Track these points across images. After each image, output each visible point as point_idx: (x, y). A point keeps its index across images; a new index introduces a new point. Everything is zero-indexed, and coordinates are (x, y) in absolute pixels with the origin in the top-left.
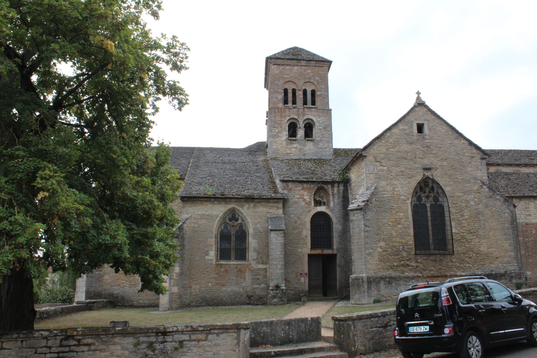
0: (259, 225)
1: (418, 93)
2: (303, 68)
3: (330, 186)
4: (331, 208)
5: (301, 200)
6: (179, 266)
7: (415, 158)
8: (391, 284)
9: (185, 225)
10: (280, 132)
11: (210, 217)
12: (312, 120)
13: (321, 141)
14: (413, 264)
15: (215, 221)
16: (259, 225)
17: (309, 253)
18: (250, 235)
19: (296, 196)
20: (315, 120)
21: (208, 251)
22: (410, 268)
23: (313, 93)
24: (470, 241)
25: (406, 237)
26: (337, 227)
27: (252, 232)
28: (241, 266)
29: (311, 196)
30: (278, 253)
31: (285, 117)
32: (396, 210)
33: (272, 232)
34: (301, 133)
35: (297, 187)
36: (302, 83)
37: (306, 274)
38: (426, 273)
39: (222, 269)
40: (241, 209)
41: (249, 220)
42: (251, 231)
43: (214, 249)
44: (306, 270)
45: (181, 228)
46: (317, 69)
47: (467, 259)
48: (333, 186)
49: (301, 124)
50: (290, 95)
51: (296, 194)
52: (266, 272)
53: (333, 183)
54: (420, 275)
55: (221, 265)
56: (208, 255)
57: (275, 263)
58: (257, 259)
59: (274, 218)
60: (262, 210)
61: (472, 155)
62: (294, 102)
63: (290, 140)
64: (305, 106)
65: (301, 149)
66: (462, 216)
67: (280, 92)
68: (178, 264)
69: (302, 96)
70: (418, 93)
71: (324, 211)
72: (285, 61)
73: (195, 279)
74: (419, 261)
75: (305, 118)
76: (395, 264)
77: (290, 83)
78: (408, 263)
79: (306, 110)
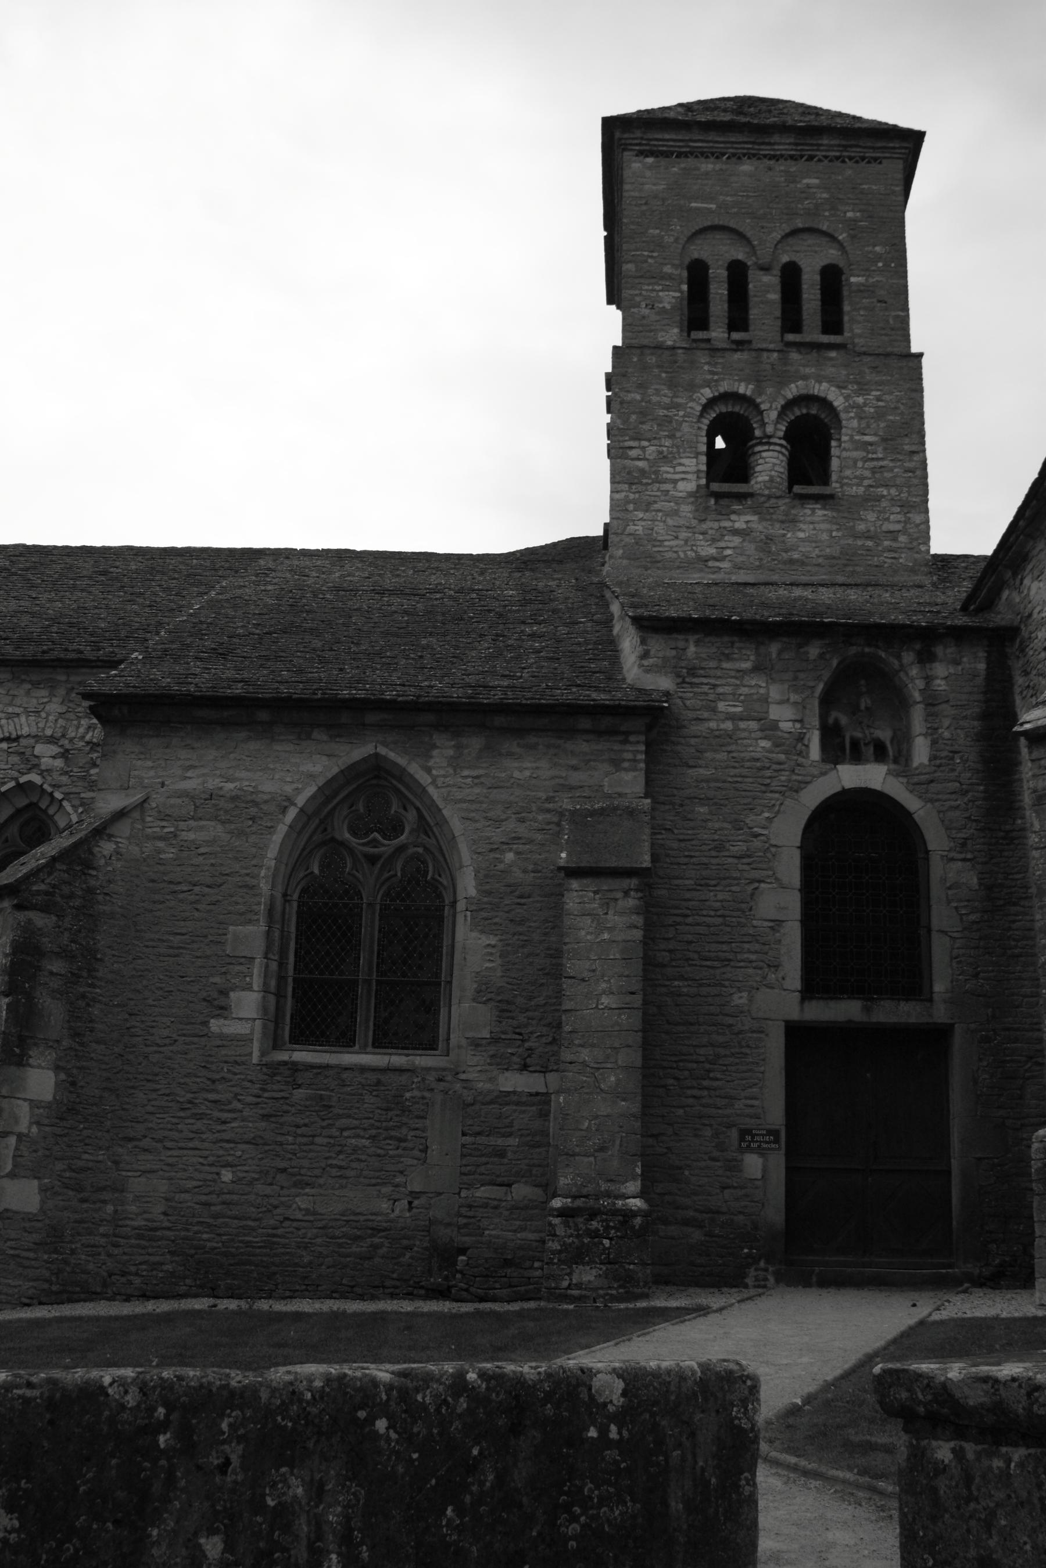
0: (510, 856)
2: (781, 166)
3: (908, 657)
4: (914, 773)
5: (753, 725)
6: (57, 1068)
9: (107, 847)
10: (663, 458)
11: (245, 811)
12: (824, 403)
13: (870, 500)
15: (271, 830)
16: (510, 856)
17: (795, 1015)
18: (461, 906)
19: (721, 706)
20: (838, 402)
21: (224, 993)
23: (832, 279)
26: (949, 874)
27: (472, 892)
28: (404, 1079)
29: (801, 706)
30: (605, 1000)
31: (692, 387)
33: (575, 884)
34: (770, 465)
35: (728, 658)
36: (777, 235)
37: (775, 1133)
39: (299, 1094)
40: (415, 769)
41: (456, 825)
42: (468, 885)
43: (257, 983)
44: (776, 1115)
45: (78, 857)
46: (849, 171)
48: (926, 658)
49: (772, 421)
50: (718, 291)
51: (721, 697)
52: (544, 1115)
53: (925, 639)
55: (295, 1067)
56: (223, 1010)
57: (585, 1055)
58: (495, 1040)
59: (592, 813)
60: (530, 771)
62: (738, 320)
63: (718, 496)
64: (790, 337)
65: (770, 538)
67: (670, 277)
68: (51, 1056)
69: (775, 296)
71: (877, 786)
73: (146, 1143)
75: (792, 391)
79: (794, 356)
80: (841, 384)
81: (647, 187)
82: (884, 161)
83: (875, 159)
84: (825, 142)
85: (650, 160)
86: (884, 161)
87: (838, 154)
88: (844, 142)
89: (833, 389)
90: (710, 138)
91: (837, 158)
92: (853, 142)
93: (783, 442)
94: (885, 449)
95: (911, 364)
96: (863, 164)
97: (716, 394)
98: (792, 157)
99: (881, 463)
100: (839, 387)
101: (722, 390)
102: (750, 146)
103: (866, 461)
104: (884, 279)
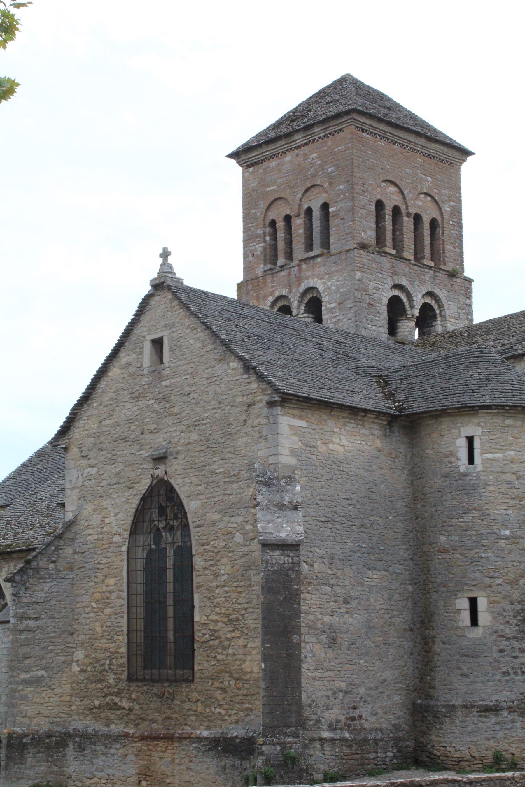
1: (165, 254)
2: (301, 151)
7: (142, 433)
8: (84, 749)
14: (125, 704)
22: (118, 712)
24: (226, 643)
25: (116, 637)
31: (265, 297)
32: (106, 571)
36: (300, 195)
38: (145, 728)
47: (217, 694)
54: (131, 732)
61: (250, 399)
66: (216, 576)
70: (165, 254)
72: (264, 149)
74: (134, 696)
76: (97, 703)
77: (275, 204)
78: (117, 700)
79: (304, 266)
83: (340, 130)
84: (316, 130)
85: (251, 169)
86: (344, 129)
87: (324, 134)
88: (323, 127)
91: (324, 136)
92: (327, 126)
93: (305, 315)
95: (351, 255)
98: (306, 144)
99: (338, 318)
100: (321, 279)
101: (276, 296)
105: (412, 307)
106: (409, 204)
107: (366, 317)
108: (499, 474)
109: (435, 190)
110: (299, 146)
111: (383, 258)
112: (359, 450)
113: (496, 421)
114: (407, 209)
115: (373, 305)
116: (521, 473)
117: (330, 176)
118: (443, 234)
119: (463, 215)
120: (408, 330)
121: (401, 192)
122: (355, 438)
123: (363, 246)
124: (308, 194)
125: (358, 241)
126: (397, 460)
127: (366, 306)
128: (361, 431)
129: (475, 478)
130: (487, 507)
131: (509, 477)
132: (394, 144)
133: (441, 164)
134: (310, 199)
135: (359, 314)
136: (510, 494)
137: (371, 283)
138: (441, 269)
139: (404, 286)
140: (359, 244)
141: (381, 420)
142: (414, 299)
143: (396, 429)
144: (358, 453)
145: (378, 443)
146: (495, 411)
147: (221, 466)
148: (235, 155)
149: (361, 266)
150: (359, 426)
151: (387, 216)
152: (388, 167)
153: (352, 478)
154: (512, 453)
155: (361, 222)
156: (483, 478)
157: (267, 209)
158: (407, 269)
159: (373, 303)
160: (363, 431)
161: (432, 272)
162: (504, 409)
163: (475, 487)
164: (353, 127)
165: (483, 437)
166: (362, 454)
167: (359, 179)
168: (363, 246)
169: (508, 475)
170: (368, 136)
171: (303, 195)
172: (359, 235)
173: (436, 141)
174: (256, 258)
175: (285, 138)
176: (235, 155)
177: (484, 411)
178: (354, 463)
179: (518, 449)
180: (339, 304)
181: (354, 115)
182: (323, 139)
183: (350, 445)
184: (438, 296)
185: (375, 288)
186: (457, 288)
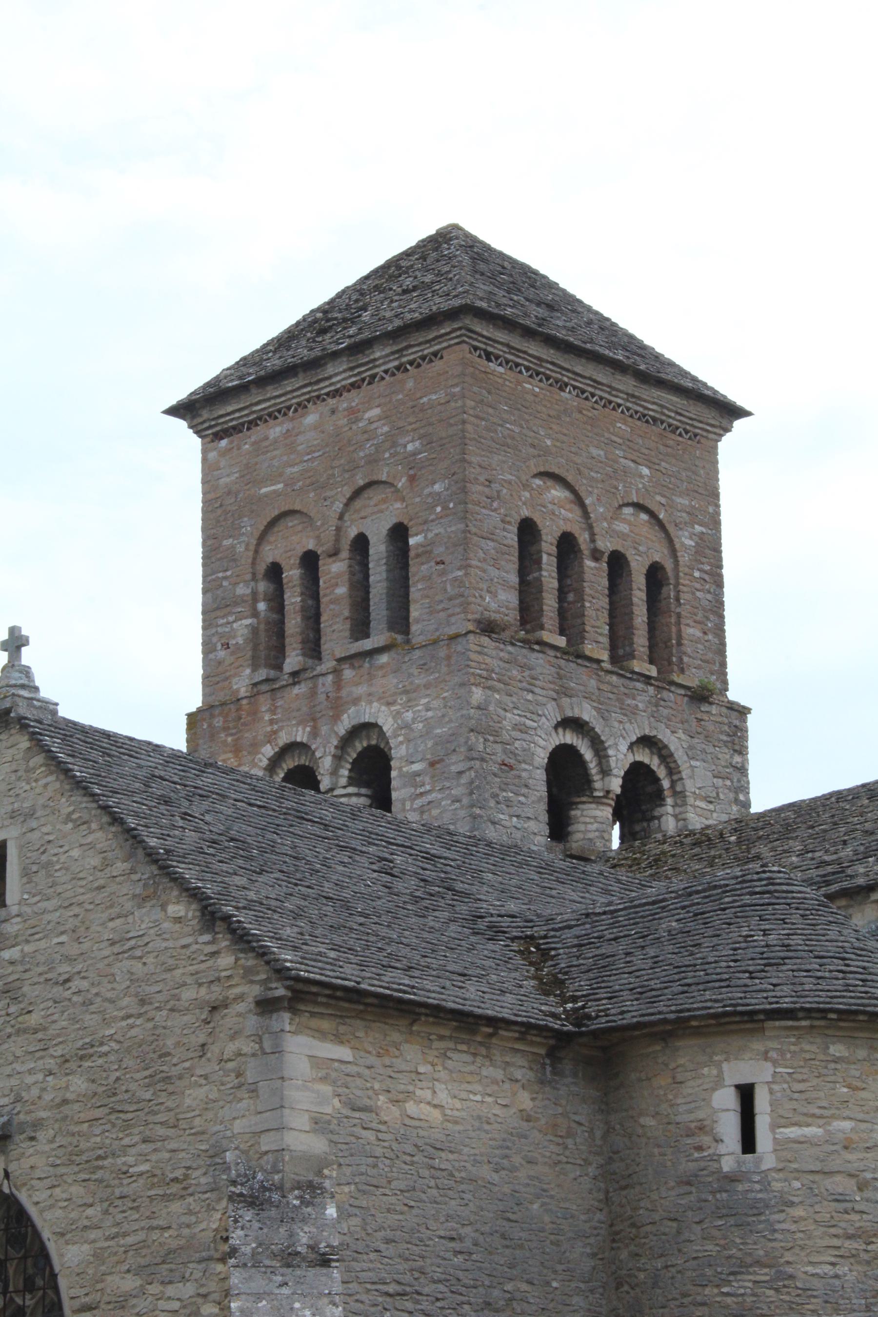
31: (255, 747)
36: (339, 506)
61: (216, 993)
72: (255, 396)
75: (344, 726)
77: (280, 526)
79: (348, 673)
80: (390, 700)
81: (223, 481)
82: (445, 353)
83: (435, 354)
84: (378, 354)
85: (224, 443)
86: (445, 353)
87: (396, 363)
88: (395, 348)
89: (383, 708)
90: (268, 395)
91: (398, 368)
92: (405, 344)
93: (351, 790)
94: (433, 777)
95: (459, 648)
96: (425, 365)
97: (277, 750)
98: (353, 385)
99: (430, 798)
100: (389, 704)
102: (309, 389)
103: (415, 799)
104: (442, 530)
105: (605, 772)
106: (597, 530)
107: (495, 796)
108: (817, 1177)
109: (658, 498)
110: (337, 391)
111: (536, 655)
112: (479, 1118)
113: (807, 1047)
114: (593, 541)
115: (511, 768)
116: (869, 1175)
117: (410, 462)
118: (678, 599)
119: (724, 555)
120: (595, 826)
121: (579, 501)
122: (470, 1087)
123: (488, 628)
124: (358, 504)
125: (477, 616)
126: (570, 1142)
127: (495, 768)
128: (484, 1072)
129: (757, 1187)
130: (788, 1256)
131: (842, 1184)
132: (561, 389)
133: (673, 436)
134: (363, 514)
135: (478, 787)
136: (842, 1224)
137: (509, 715)
138: (672, 683)
139: (587, 723)
140: (479, 622)
141: (532, 1043)
142: (611, 752)
143: (567, 1066)
144: (477, 1124)
145: (525, 1100)
146: (804, 1023)
147: (144, 1157)
148: (184, 410)
149: (484, 673)
150: (479, 1059)
151: (545, 557)
152: (549, 442)
153: (463, 1187)
154: (847, 1125)
155: (484, 571)
156: (777, 1186)
157: (262, 538)
158: (593, 683)
159: (512, 762)
160: (489, 1071)
161: (651, 689)
162: (825, 1018)
163: (758, 1208)
164: (465, 347)
165: (776, 1087)
166: (487, 1127)
167: (478, 470)
168: (488, 628)
169: (838, 1178)
170: (501, 369)
171: (347, 505)
172: (479, 600)
173: (661, 383)
174: (233, 653)
175: (305, 371)
176: (184, 410)
177: (777, 1023)
178: (466, 1150)
179: (861, 1116)
180: (432, 764)
181: (468, 321)
182: (393, 375)
183: (458, 1105)
184: (666, 747)
185: (516, 727)
186: (711, 727)
